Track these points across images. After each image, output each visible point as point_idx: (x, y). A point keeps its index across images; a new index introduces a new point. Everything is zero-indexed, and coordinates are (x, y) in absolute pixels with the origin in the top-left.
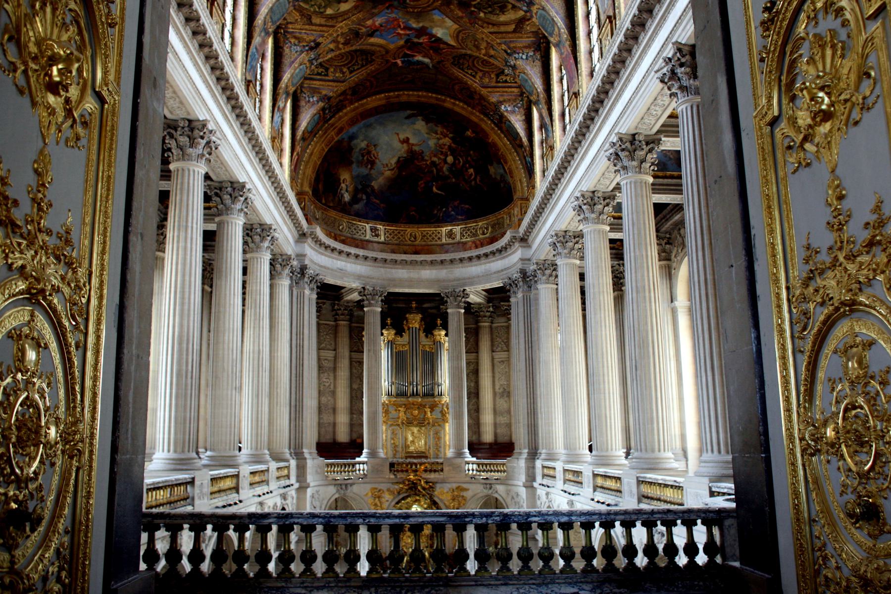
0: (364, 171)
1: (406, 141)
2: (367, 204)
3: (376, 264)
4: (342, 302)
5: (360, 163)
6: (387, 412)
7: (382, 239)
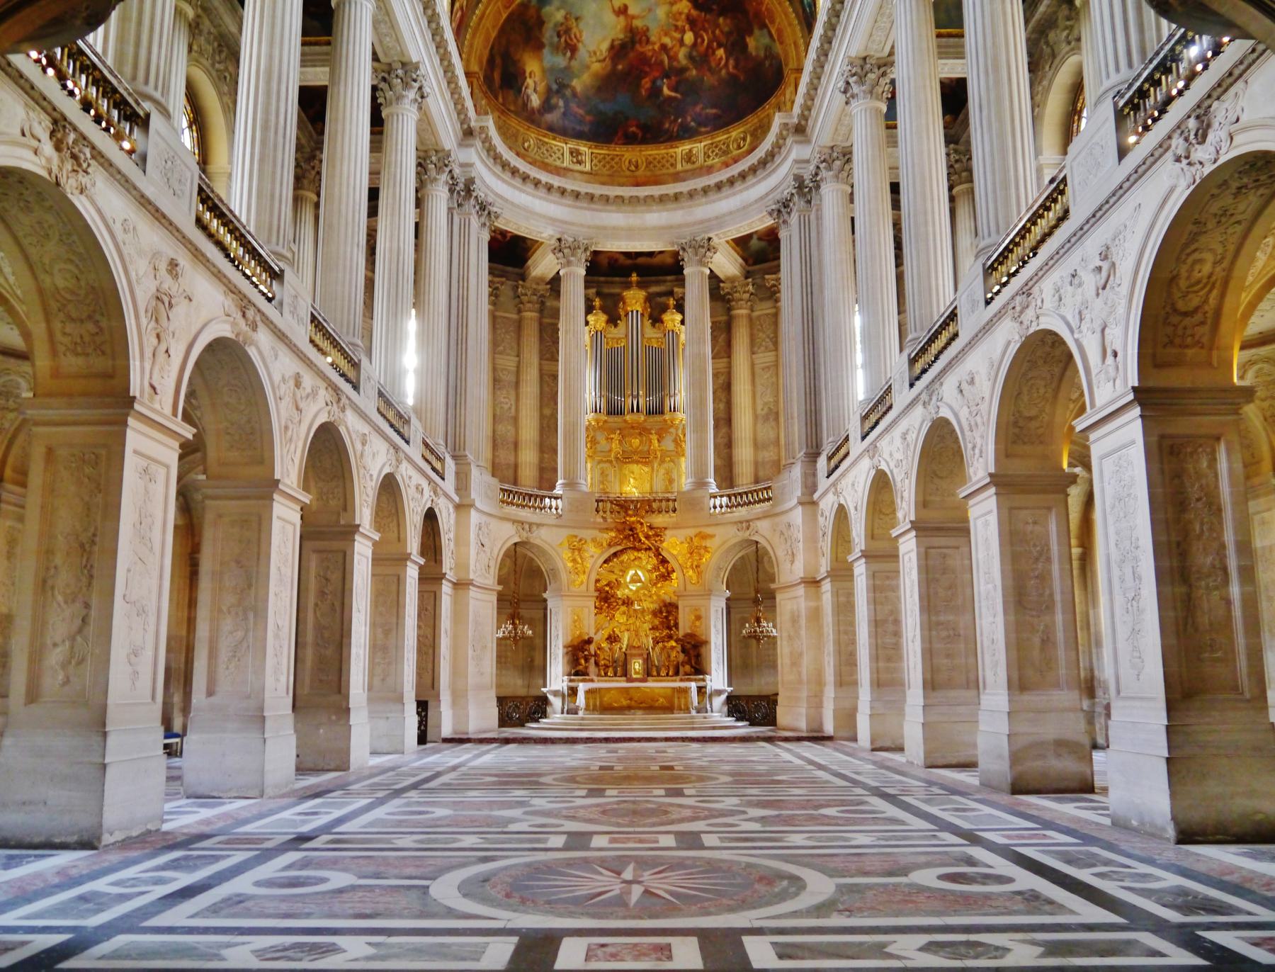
0: (561, 61)
1: (623, 11)
2: (564, 114)
3: (578, 204)
4: (528, 284)
5: (556, 49)
6: (593, 442)
7: (588, 168)
